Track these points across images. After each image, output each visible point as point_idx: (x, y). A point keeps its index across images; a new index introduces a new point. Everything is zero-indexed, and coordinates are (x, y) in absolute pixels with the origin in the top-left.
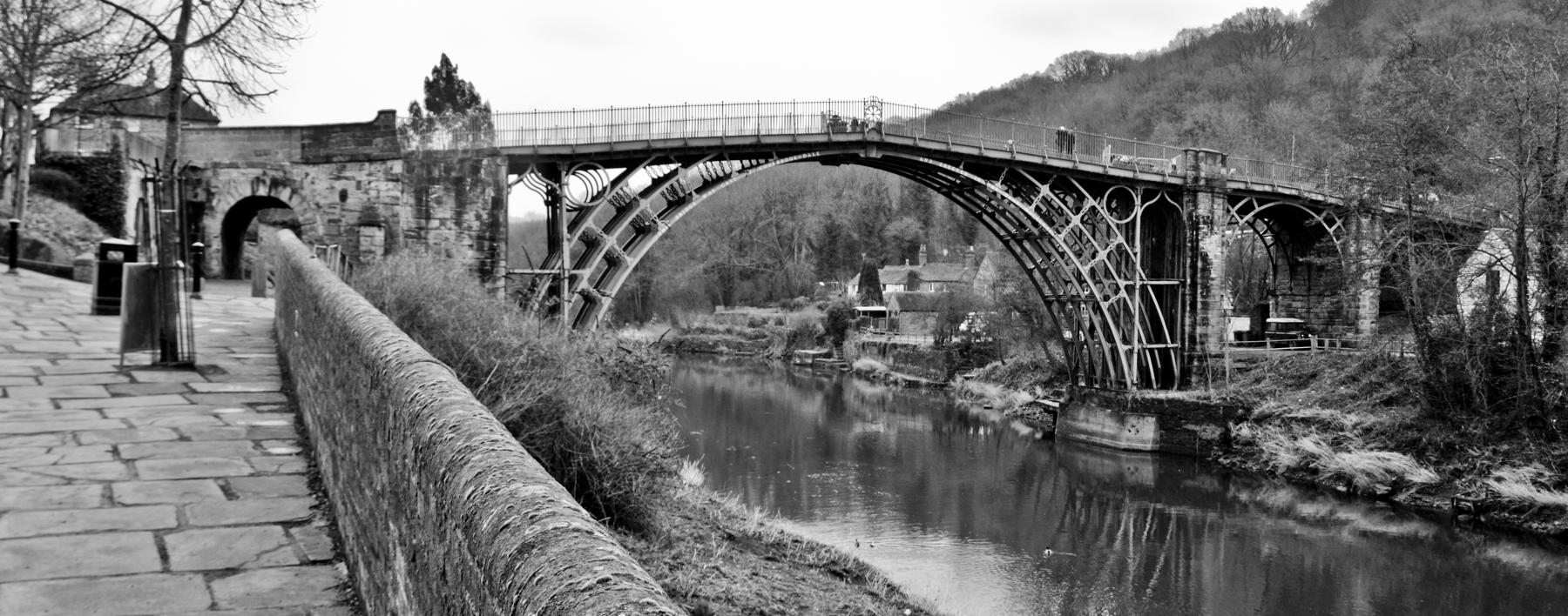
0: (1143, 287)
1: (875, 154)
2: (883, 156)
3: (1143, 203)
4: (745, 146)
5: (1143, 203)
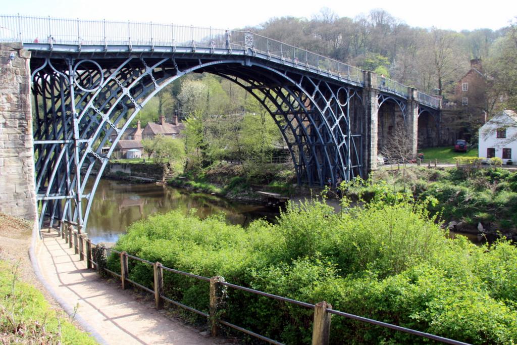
0: (351, 137)
1: (249, 64)
2: (253, 65)
3: (350, 96)
4: (186, 54)
5: (350, 96)
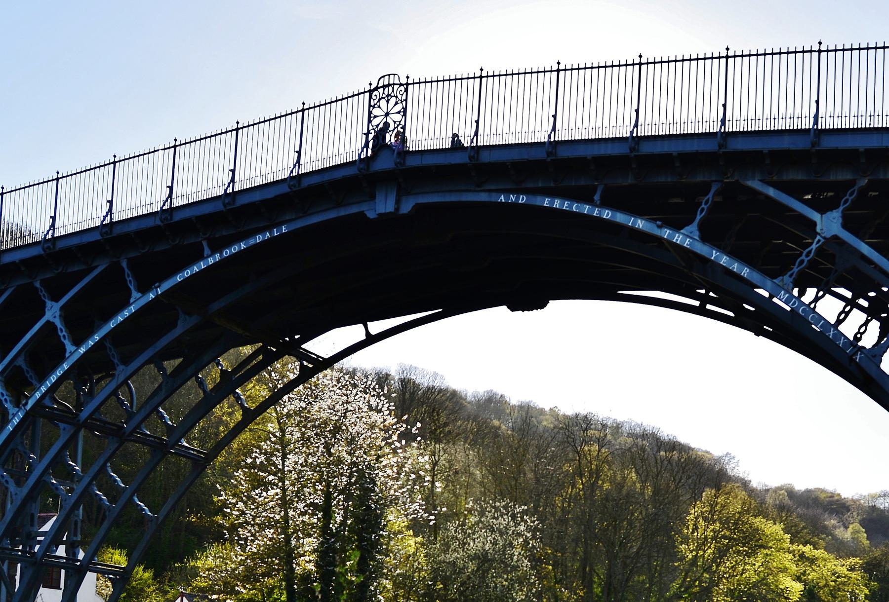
2: (418, 207)
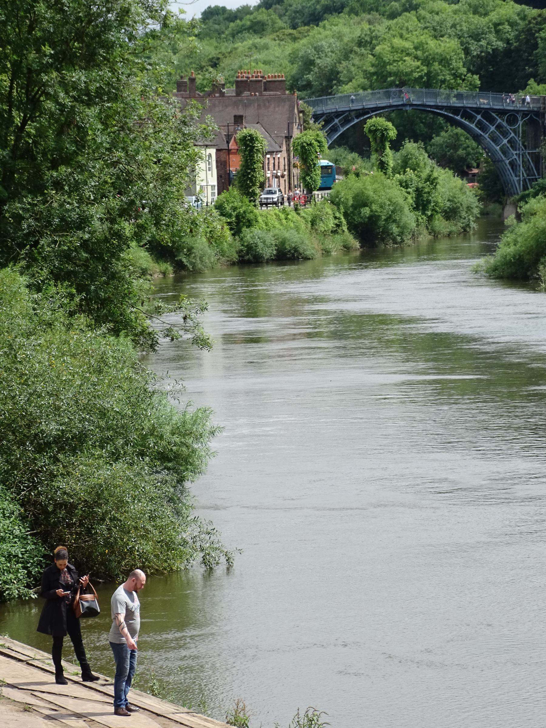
3: (522, 119)
5: (522, 119)
